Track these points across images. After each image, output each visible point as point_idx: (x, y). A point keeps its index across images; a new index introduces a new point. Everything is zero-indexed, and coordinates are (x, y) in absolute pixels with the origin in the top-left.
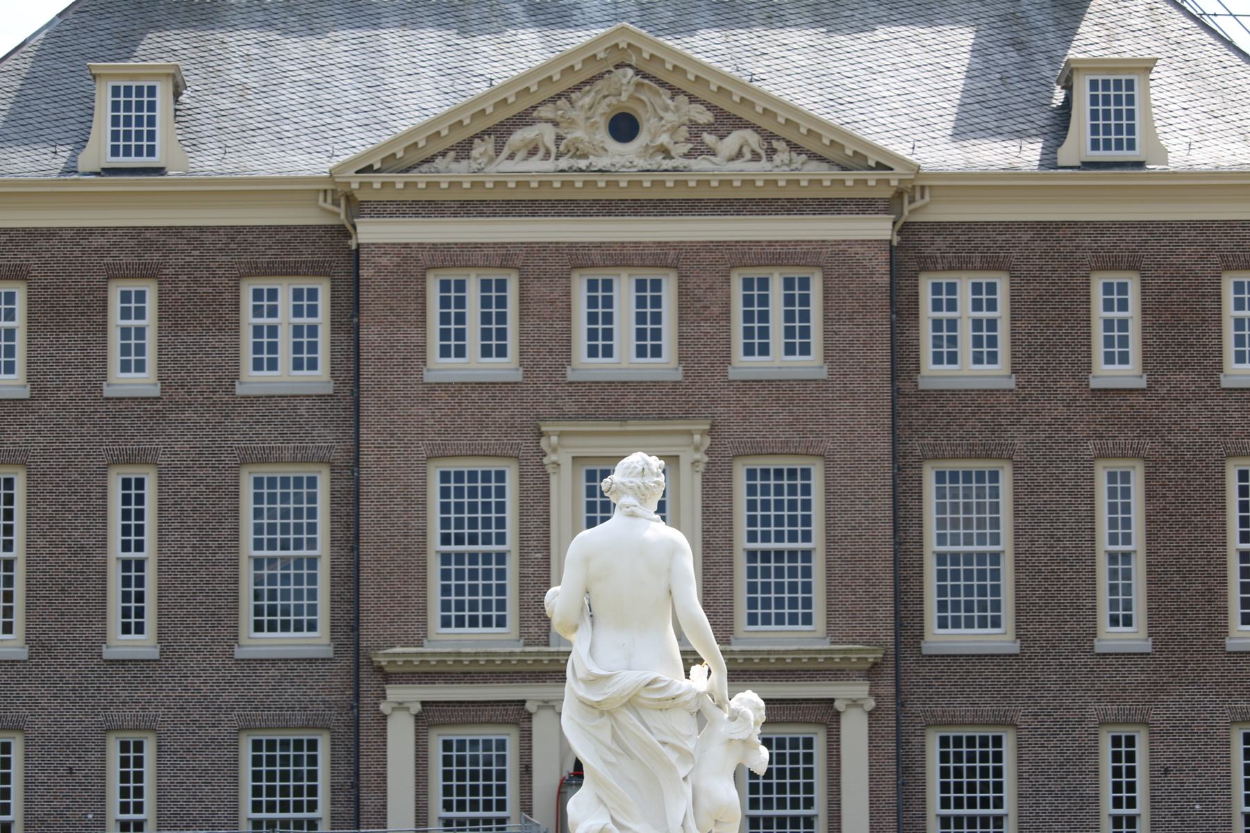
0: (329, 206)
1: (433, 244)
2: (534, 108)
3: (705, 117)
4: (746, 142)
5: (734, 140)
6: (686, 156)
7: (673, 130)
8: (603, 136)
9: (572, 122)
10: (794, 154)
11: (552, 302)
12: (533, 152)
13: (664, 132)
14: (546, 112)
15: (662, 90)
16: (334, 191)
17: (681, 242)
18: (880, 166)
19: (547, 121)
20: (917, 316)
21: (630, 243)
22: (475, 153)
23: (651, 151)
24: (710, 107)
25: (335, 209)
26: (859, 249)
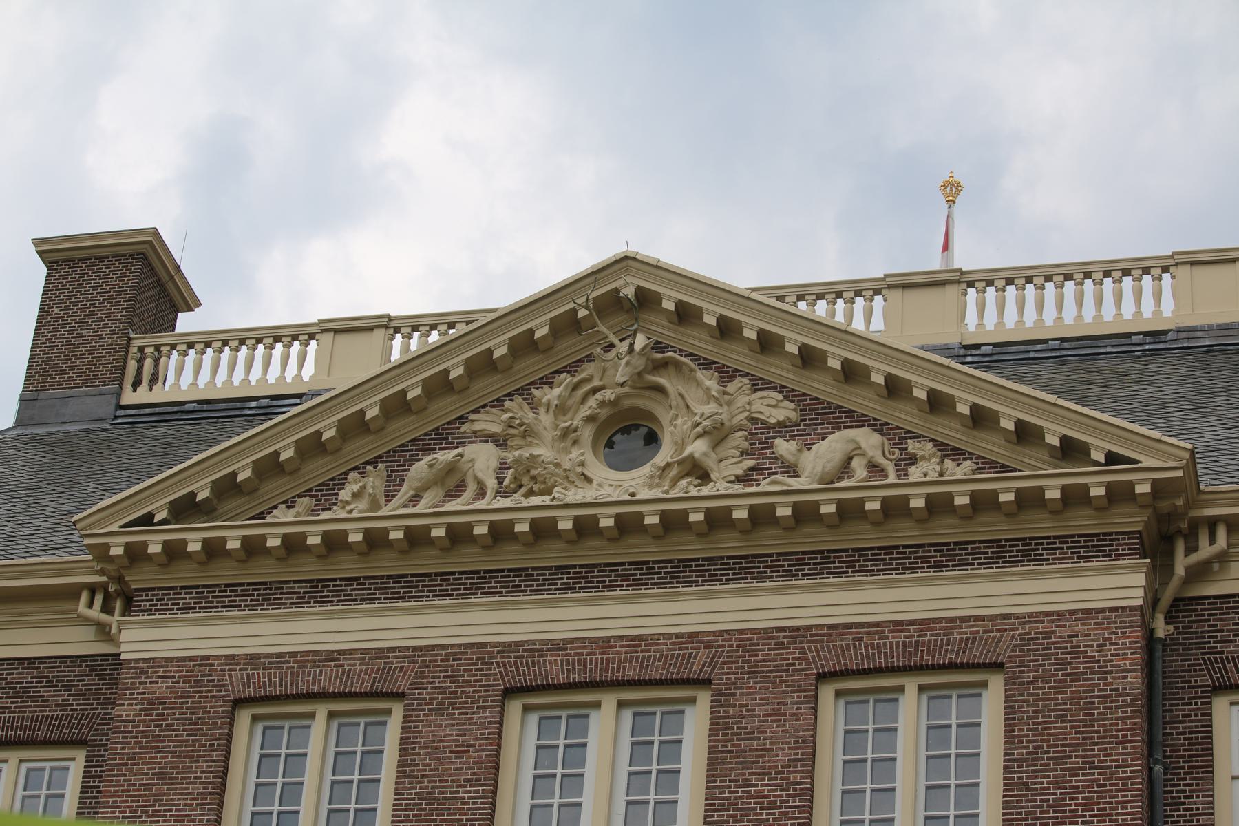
0: (95, 613)
1: (253, 657)
2: (463, 419)
3: (785, 412)
4: (857, 450)
5: (831, 448)
6: (739, 479)
7: (717, 434)
8: (585, 454)
9: (528, 433)
10: (949, 464)
11: (459, 752)
12: (457, 491)
13: (699, 436)
14: (490, 423)
15: (700, 374)
16: (104, 587)
17: (722, 632)
18: (1112, 458)
19: (487, 438)
20: (1209, 770)
21: (621, 638)
22: (344, 495)
23: (674, 472)
24: (790, 394)
25: (104, 617)
26: (1079, 628)
